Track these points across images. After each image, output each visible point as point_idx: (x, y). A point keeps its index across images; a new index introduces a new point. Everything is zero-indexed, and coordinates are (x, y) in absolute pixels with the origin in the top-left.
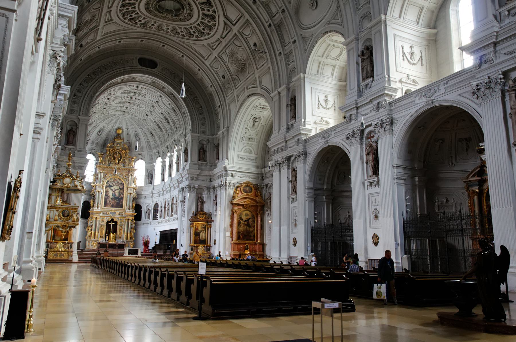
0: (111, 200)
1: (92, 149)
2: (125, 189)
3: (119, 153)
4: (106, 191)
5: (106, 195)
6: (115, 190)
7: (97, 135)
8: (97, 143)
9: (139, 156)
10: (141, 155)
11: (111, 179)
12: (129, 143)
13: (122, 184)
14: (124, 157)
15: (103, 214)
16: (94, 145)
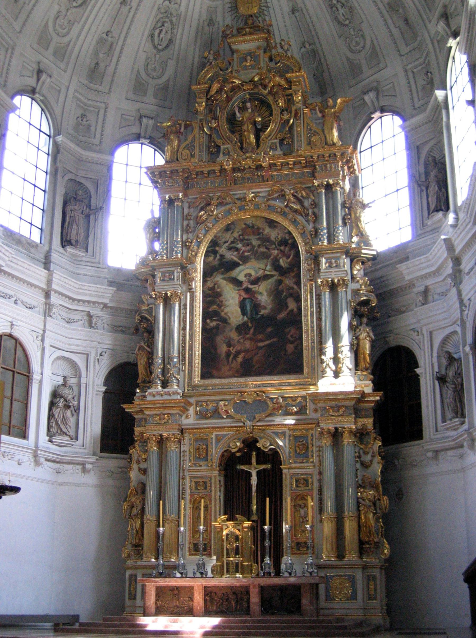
0: (234, 336)
1: (141, 117)
2: (304, 266)
3: (253, 97)
4: (205, 296)
5: (206, 315)
6: (256, 281)
7: (149, 46)
8: (165, 88)
9: (369, 98)
10: (377, 90)
11: (228, 228)
12: (314, 53)
13: (284, 242)
14: (282, 111)
15: (202, 415)
16: (150, 98)
